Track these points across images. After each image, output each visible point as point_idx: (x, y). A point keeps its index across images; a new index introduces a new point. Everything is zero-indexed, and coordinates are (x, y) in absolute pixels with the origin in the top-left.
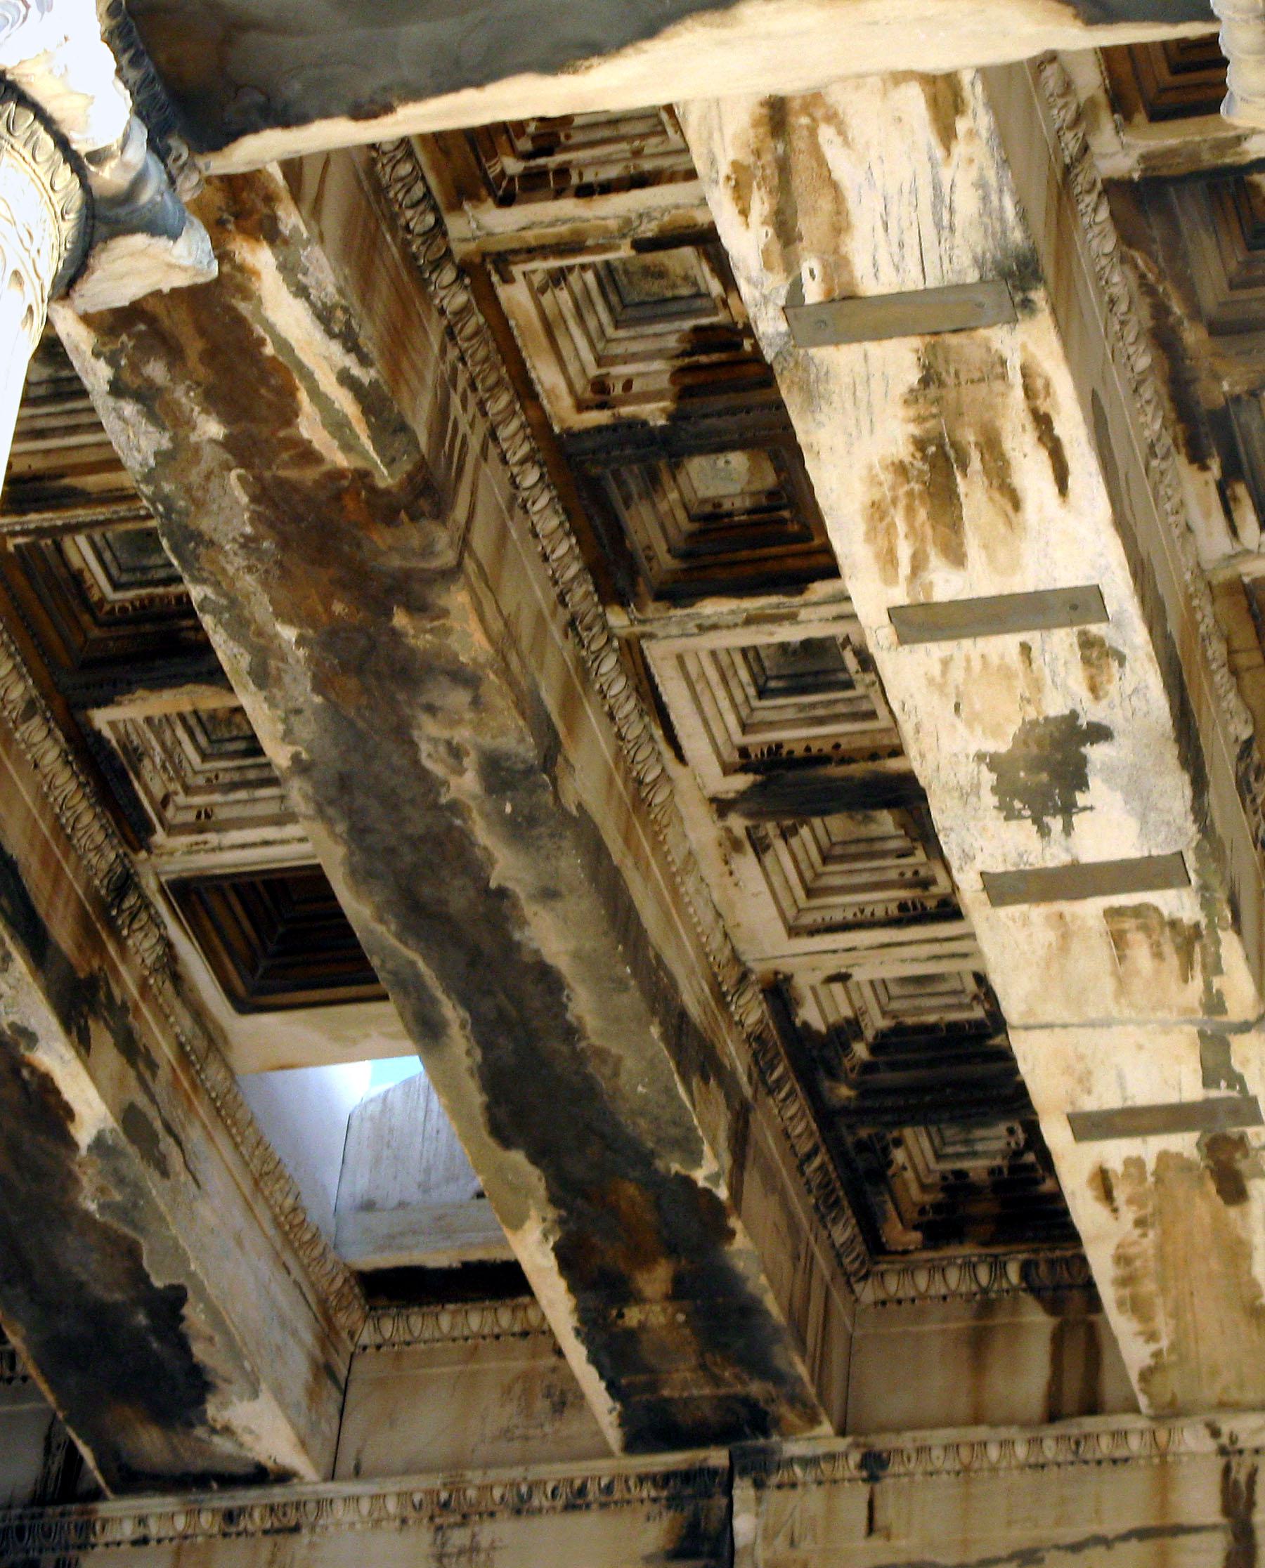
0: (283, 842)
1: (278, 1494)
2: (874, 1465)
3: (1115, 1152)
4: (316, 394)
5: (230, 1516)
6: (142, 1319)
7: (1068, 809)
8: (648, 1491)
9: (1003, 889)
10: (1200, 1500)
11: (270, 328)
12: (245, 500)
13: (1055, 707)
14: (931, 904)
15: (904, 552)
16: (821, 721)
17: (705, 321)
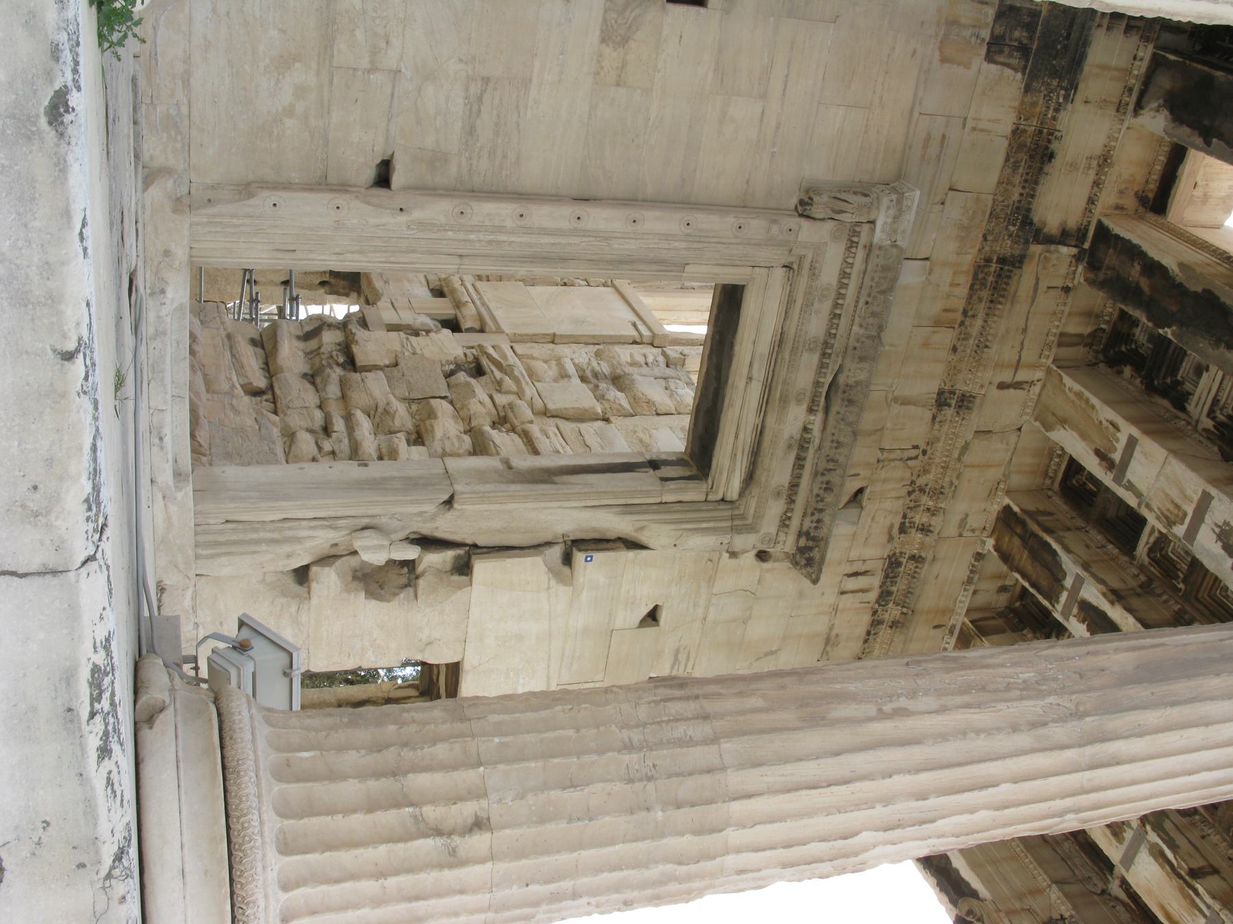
2: (1067, 290)
3: (1123, 439)
7: (1220, 537)
8: (1085, 223)
9: (1206, 499)
10: (1022, 376)
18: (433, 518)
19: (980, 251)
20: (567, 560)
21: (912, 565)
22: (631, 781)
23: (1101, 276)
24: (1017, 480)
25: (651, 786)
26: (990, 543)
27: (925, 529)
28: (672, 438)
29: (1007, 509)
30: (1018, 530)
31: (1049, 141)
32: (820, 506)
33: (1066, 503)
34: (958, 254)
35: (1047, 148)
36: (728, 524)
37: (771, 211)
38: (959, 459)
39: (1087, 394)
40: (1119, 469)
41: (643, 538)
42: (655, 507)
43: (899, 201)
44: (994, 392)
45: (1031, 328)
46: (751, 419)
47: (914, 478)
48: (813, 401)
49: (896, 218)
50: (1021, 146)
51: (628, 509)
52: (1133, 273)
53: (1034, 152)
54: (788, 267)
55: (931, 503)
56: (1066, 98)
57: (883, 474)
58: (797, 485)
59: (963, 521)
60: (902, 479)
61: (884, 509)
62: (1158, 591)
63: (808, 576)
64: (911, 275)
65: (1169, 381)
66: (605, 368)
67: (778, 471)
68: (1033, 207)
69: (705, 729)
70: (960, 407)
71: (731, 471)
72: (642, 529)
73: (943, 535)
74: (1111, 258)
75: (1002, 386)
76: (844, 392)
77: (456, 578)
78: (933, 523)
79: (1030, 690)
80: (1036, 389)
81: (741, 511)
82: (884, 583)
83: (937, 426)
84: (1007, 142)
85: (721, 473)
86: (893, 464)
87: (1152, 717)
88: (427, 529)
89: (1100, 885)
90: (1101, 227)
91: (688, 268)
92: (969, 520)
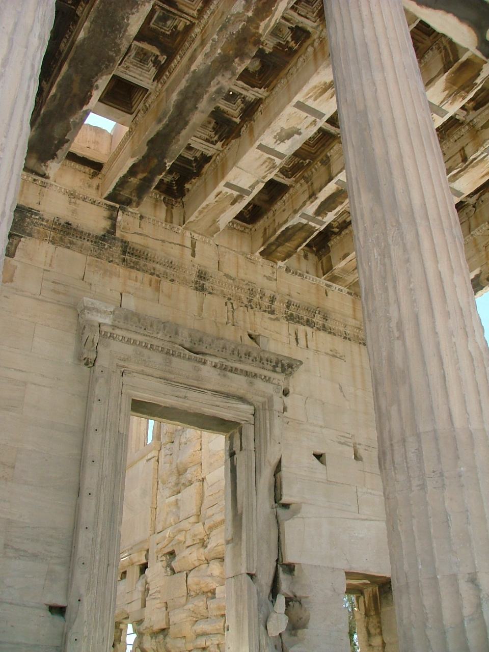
0: (138, 79)
1: (44, 180)
2: (142, 217)
4: (270, 20)
5: (35, 180)
6: (56, 142)
7: (282, 141)
9: (261, 147)
10: (188, 243)
11: (277, 6)
12: (240, 27)
13: (299, 127)
14: (211, 140)
15: (310, 95)
16: (227, 107)
17: (281, 42)
18: (261, 586)
19: (118, 265)
20: (286, 506)
21: (292, 307)
22: (443, 486)
23: (135, 199)
24: (246, 249)
25: (446, 474)
26: (280, 263)
27: (272, 300)
28: (217, 442)
29: (261, 253)
30: (274, 247)
31: (60, 224)
32: (258, 359)
33: (259, 221)
34: (119, 277)
35: (63, 225)
37: (91, 382)
39: (200, 208)
40: (243, 192)
41: (274, 462)
42: (257, 455)
43: (89, 309)
44: (197, 259)
45: (162, 238)
46: (208, 397)
47: (243, 305)
48: (199, 362)
49: (98, 311)
50: (61, 239)
51: (258, 470)
52: (135, 182)
53: (65, 232)
55: (258, 296)
56: (36, 214)
59: (269, 278)
60: (244, 312)
61: (262, 323)
62: (310, 173)
63: (298, 366)
64: (130, 303)
65: (194, 165)
66: (173, 479)
67: (238, 384)
68: (95, 234)
69: (411, 440)
70: (204, 278)
72: (269, 462)
73: (275, 289)
74: (125, 193)
75: (193, 255)
77: (296, 573)
78: (269, 295)
79: (385, 254)
80: (196, 236)
82: (302, 324)
83: (215, 292)
85: (239, 416)
86: (235, 317)
87: (399, 185)
88: (267, 590)
89: (471, 208)
90: (109, 198)
91: (121, 431)
92: (267, 275)
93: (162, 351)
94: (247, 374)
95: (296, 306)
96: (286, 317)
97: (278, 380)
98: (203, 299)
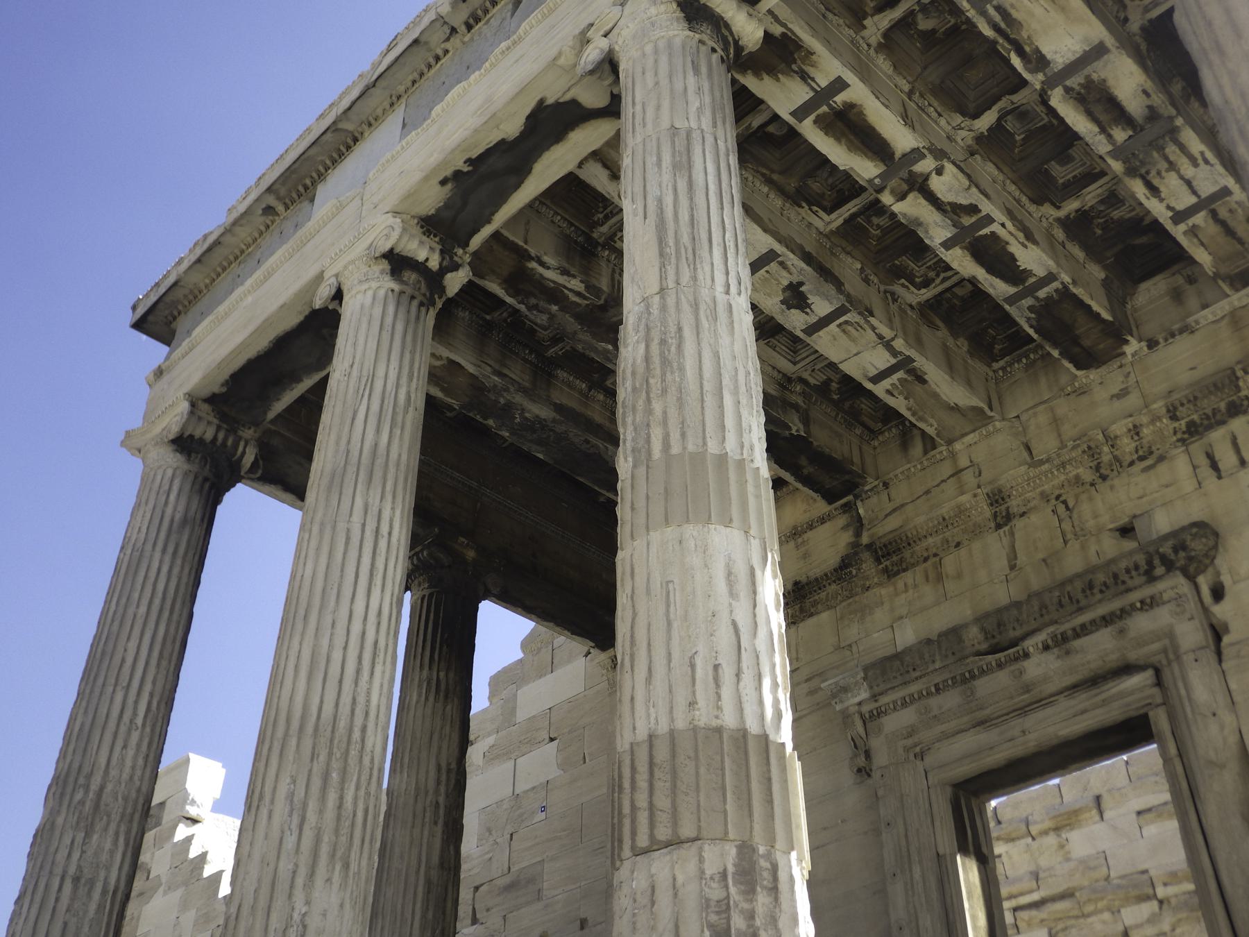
3: (886, 383)
7: (809, 306)
13: (786, 283)
19: (880, 584)
21: (1182, 412)
23: (847, 477)
27: (1136, 431)
32: (1110, 581)
34: (882, 603)
36: (1175, 666)
38: (1048, 461)
44: (986, 476)
46: (1065, 705)
50: (802, 610)
54: (921, 756)
55: (1106, 449)
57: (1091, 524)
58: (1103, 618)
59: (1122, 394)
67: (1099, 648)
71: (1122, 695)
76: (993, 637)
81: (1162, 657)
83: (1032, 504)
84: (801, 625)
92: (1115, 391)
93: (954, 684)
94: (1107, 620)
95: (1189, 401)
96: (1178, 440)
97: (1172, 588)
98: (1012, 534)
